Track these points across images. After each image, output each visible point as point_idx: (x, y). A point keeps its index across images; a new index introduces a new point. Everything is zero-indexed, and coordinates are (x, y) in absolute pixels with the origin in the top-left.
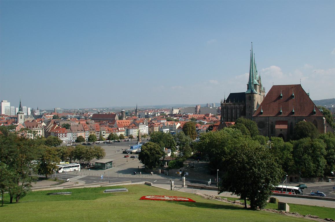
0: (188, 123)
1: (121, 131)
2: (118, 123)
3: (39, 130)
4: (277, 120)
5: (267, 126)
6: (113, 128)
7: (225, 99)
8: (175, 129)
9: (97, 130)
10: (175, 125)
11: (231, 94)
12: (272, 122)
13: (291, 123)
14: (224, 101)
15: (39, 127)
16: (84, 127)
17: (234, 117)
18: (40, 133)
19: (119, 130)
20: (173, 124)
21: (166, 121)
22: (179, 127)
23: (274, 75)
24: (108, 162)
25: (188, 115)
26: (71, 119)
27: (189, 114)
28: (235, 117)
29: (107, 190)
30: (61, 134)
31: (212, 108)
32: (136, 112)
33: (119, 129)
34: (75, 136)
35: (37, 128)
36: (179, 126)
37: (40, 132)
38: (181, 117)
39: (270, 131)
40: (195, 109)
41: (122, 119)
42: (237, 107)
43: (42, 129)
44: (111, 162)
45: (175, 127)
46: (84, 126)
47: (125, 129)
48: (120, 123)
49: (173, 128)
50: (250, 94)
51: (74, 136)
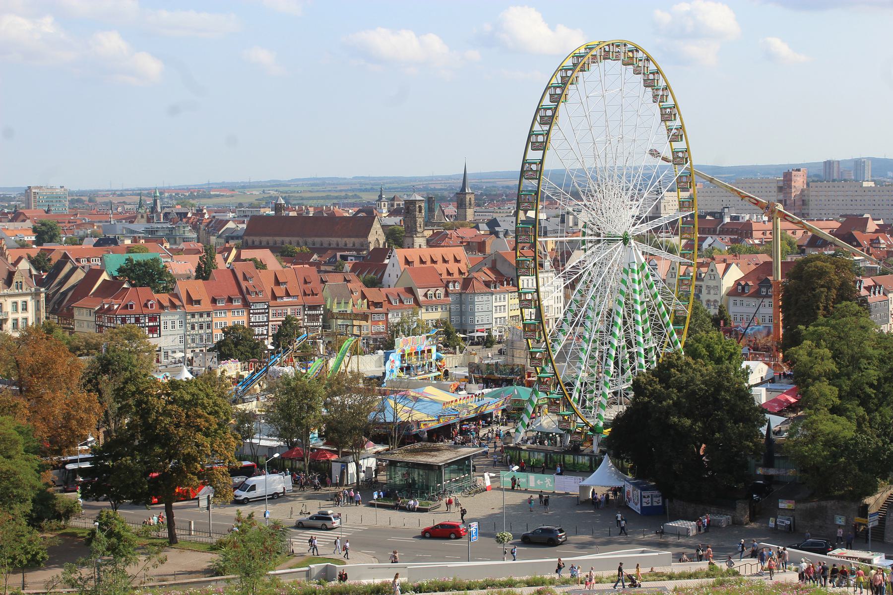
0: (819, 264)
1: (431, 306)
2: (403, 266)
3: (20, 300)
6: (384, 291)
8: (712, 298)
9: (310, 300)
10: (713, 276)
15: (20, 286)
16: (244, 285)
18: (25, 315)
19: (421, 298)
20: (704, 270)
22: (738, 290)
24: (450, 464)
25: (748, 224)
26: (135, 240)
27: (747, 217)
30: (133, 320)
31: (872, 184)
32: (461, 205)
33: (420, 292)
34: (201, 327)
35: (13, 290)
36: (737, 283)
37: (25, 309)
38: (713, 232)
40: (780, 189)
41: (408, 241)
43: (37, 294)
45: (712, 283)
46: (240, 277)
47: (447, 294)
48: (417, 264)
49: (704, 290)
51: (193, 328)
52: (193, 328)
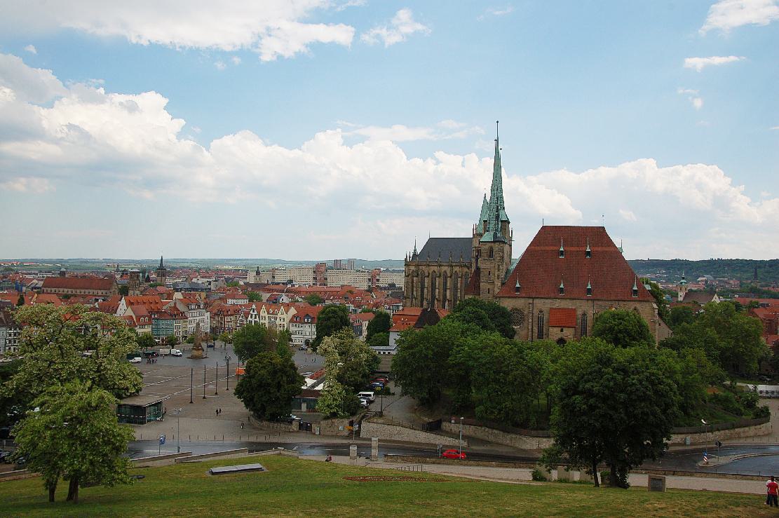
4: (554, 307)
5: (530, 321)
7: (415, 250)
11: (431, 239)
12: (541, 312)
13: (584, 314)
14: (415, 255)
17: (437, 297)
21: (246, 302)
23: (542, 202)
28: (441, 298)
29: (215, 470)
39: (536, 329)
42: (445, 272)
44: (158, 404)
49: (278, 319)
50: (492, 244)
51: (10, 335)
52: (10, 335)
